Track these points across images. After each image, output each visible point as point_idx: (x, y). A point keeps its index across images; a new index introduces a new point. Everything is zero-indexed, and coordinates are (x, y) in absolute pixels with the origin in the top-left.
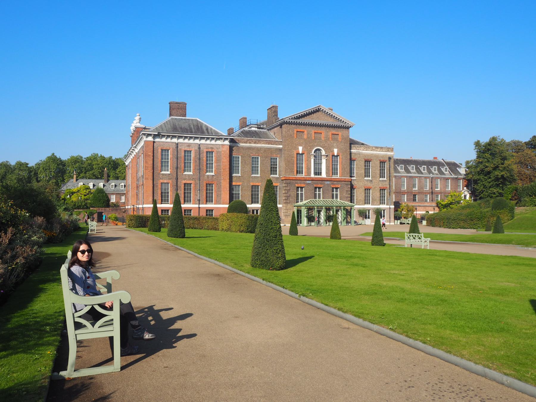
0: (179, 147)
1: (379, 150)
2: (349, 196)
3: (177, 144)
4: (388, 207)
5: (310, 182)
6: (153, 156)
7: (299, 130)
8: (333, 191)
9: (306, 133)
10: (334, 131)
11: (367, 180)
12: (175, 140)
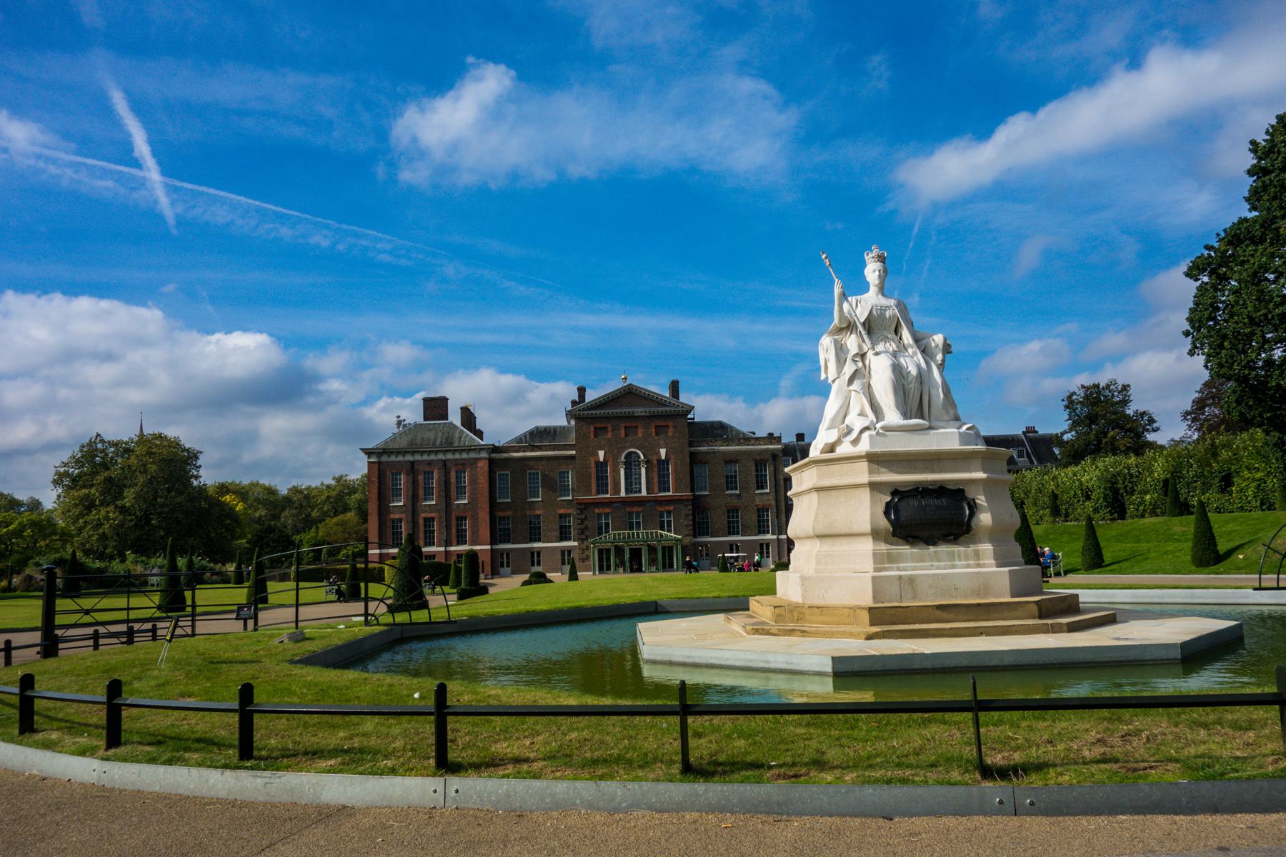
3: (412, 463)
10: (659, 422)
11: (731, 495)
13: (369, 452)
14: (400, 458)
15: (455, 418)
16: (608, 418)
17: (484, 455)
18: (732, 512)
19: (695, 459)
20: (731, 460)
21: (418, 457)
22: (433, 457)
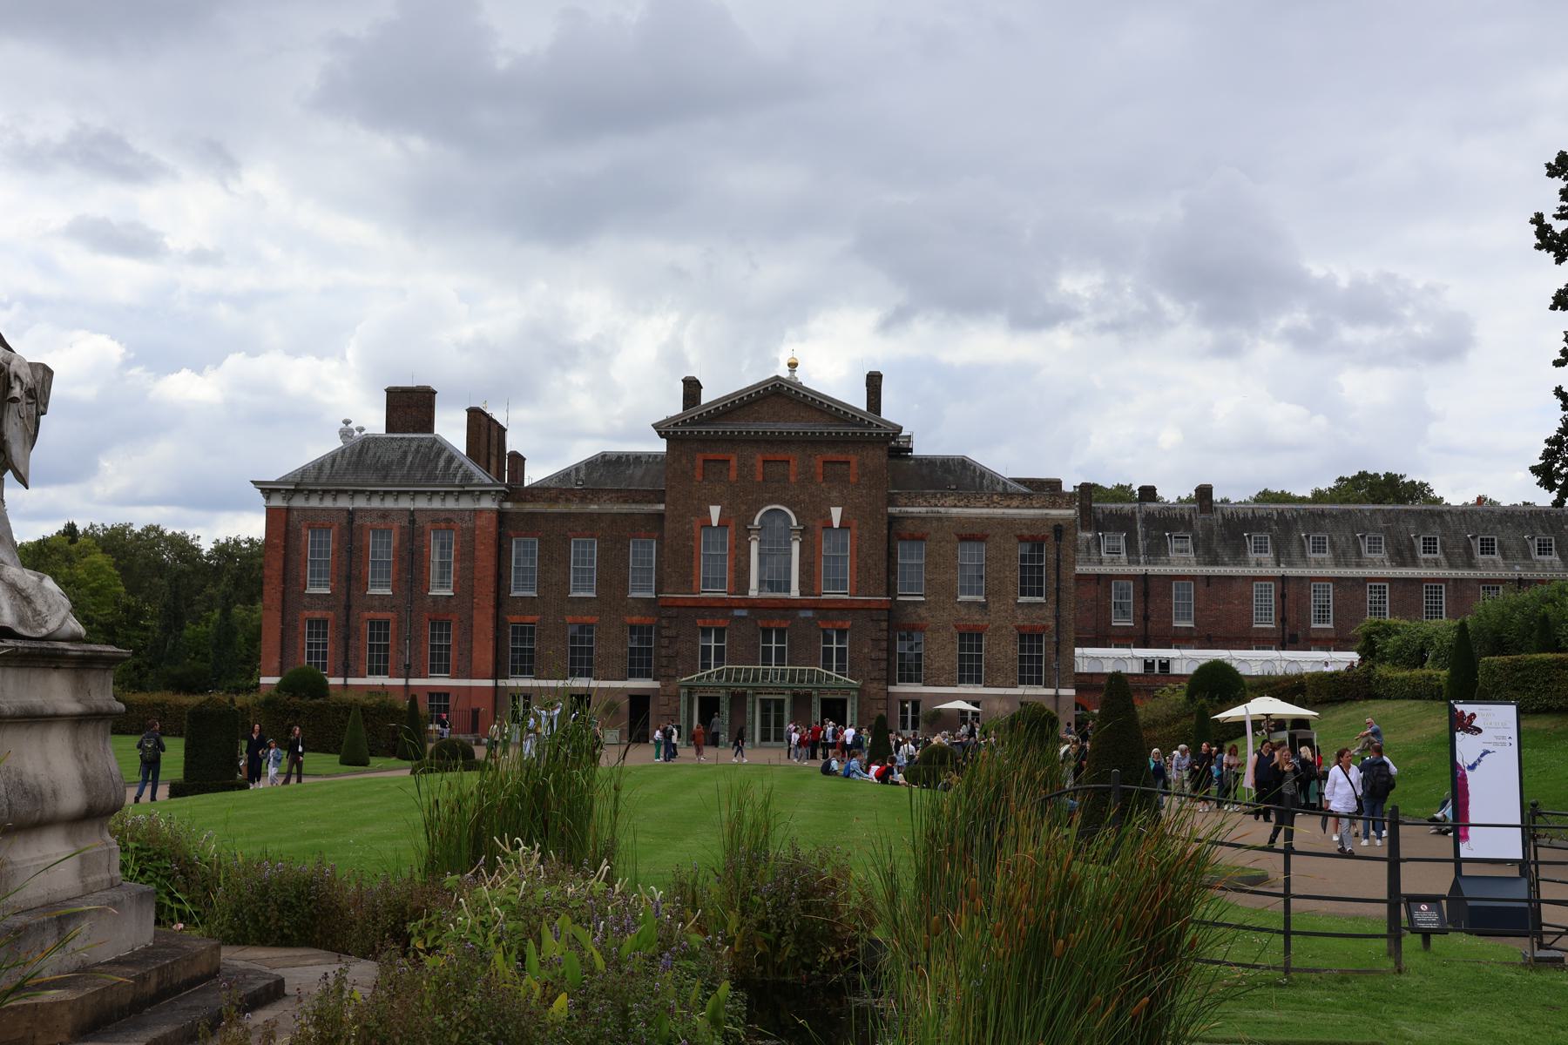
0: (358, 521)
1: (1015, 503)
2: (885, 656)
3: (351, 513)
4: (1051, 692)
5: (744, 613)
6: (285, 548)
7: (711, 456)
8: (828, 640)
9: (734, 462)
10: (832, 455)
11: (970, 604)
12: (344, 503)
13: (268, 489)
14: (328, 503)
15: (451, 429)
16: (733, 440)
17: (487, 503)
18: (970, 637)
19: (896, 531)
20: (972, 534)
21: (360, 503)
22: (389, 504)
